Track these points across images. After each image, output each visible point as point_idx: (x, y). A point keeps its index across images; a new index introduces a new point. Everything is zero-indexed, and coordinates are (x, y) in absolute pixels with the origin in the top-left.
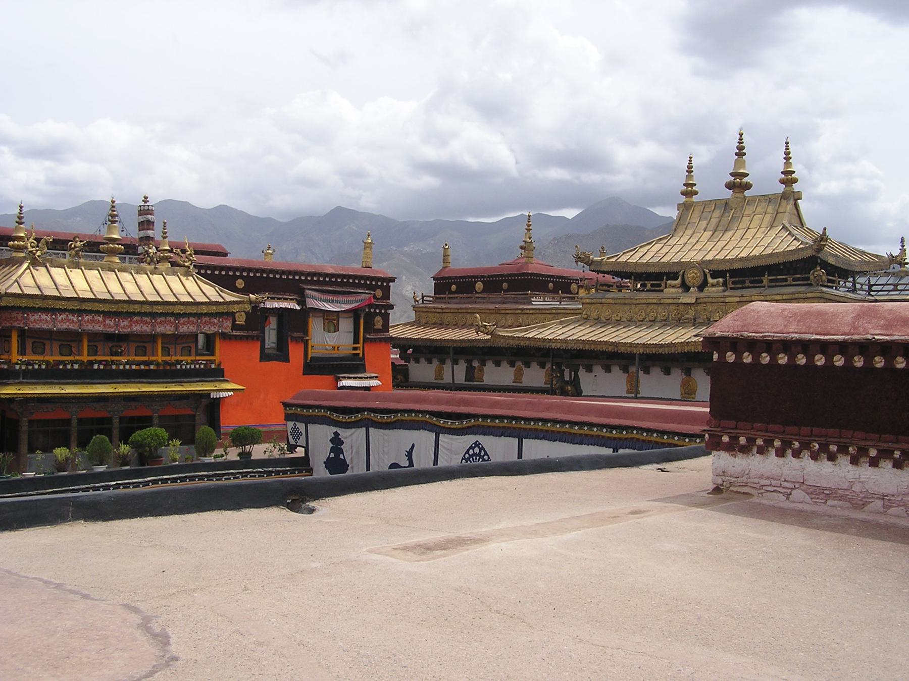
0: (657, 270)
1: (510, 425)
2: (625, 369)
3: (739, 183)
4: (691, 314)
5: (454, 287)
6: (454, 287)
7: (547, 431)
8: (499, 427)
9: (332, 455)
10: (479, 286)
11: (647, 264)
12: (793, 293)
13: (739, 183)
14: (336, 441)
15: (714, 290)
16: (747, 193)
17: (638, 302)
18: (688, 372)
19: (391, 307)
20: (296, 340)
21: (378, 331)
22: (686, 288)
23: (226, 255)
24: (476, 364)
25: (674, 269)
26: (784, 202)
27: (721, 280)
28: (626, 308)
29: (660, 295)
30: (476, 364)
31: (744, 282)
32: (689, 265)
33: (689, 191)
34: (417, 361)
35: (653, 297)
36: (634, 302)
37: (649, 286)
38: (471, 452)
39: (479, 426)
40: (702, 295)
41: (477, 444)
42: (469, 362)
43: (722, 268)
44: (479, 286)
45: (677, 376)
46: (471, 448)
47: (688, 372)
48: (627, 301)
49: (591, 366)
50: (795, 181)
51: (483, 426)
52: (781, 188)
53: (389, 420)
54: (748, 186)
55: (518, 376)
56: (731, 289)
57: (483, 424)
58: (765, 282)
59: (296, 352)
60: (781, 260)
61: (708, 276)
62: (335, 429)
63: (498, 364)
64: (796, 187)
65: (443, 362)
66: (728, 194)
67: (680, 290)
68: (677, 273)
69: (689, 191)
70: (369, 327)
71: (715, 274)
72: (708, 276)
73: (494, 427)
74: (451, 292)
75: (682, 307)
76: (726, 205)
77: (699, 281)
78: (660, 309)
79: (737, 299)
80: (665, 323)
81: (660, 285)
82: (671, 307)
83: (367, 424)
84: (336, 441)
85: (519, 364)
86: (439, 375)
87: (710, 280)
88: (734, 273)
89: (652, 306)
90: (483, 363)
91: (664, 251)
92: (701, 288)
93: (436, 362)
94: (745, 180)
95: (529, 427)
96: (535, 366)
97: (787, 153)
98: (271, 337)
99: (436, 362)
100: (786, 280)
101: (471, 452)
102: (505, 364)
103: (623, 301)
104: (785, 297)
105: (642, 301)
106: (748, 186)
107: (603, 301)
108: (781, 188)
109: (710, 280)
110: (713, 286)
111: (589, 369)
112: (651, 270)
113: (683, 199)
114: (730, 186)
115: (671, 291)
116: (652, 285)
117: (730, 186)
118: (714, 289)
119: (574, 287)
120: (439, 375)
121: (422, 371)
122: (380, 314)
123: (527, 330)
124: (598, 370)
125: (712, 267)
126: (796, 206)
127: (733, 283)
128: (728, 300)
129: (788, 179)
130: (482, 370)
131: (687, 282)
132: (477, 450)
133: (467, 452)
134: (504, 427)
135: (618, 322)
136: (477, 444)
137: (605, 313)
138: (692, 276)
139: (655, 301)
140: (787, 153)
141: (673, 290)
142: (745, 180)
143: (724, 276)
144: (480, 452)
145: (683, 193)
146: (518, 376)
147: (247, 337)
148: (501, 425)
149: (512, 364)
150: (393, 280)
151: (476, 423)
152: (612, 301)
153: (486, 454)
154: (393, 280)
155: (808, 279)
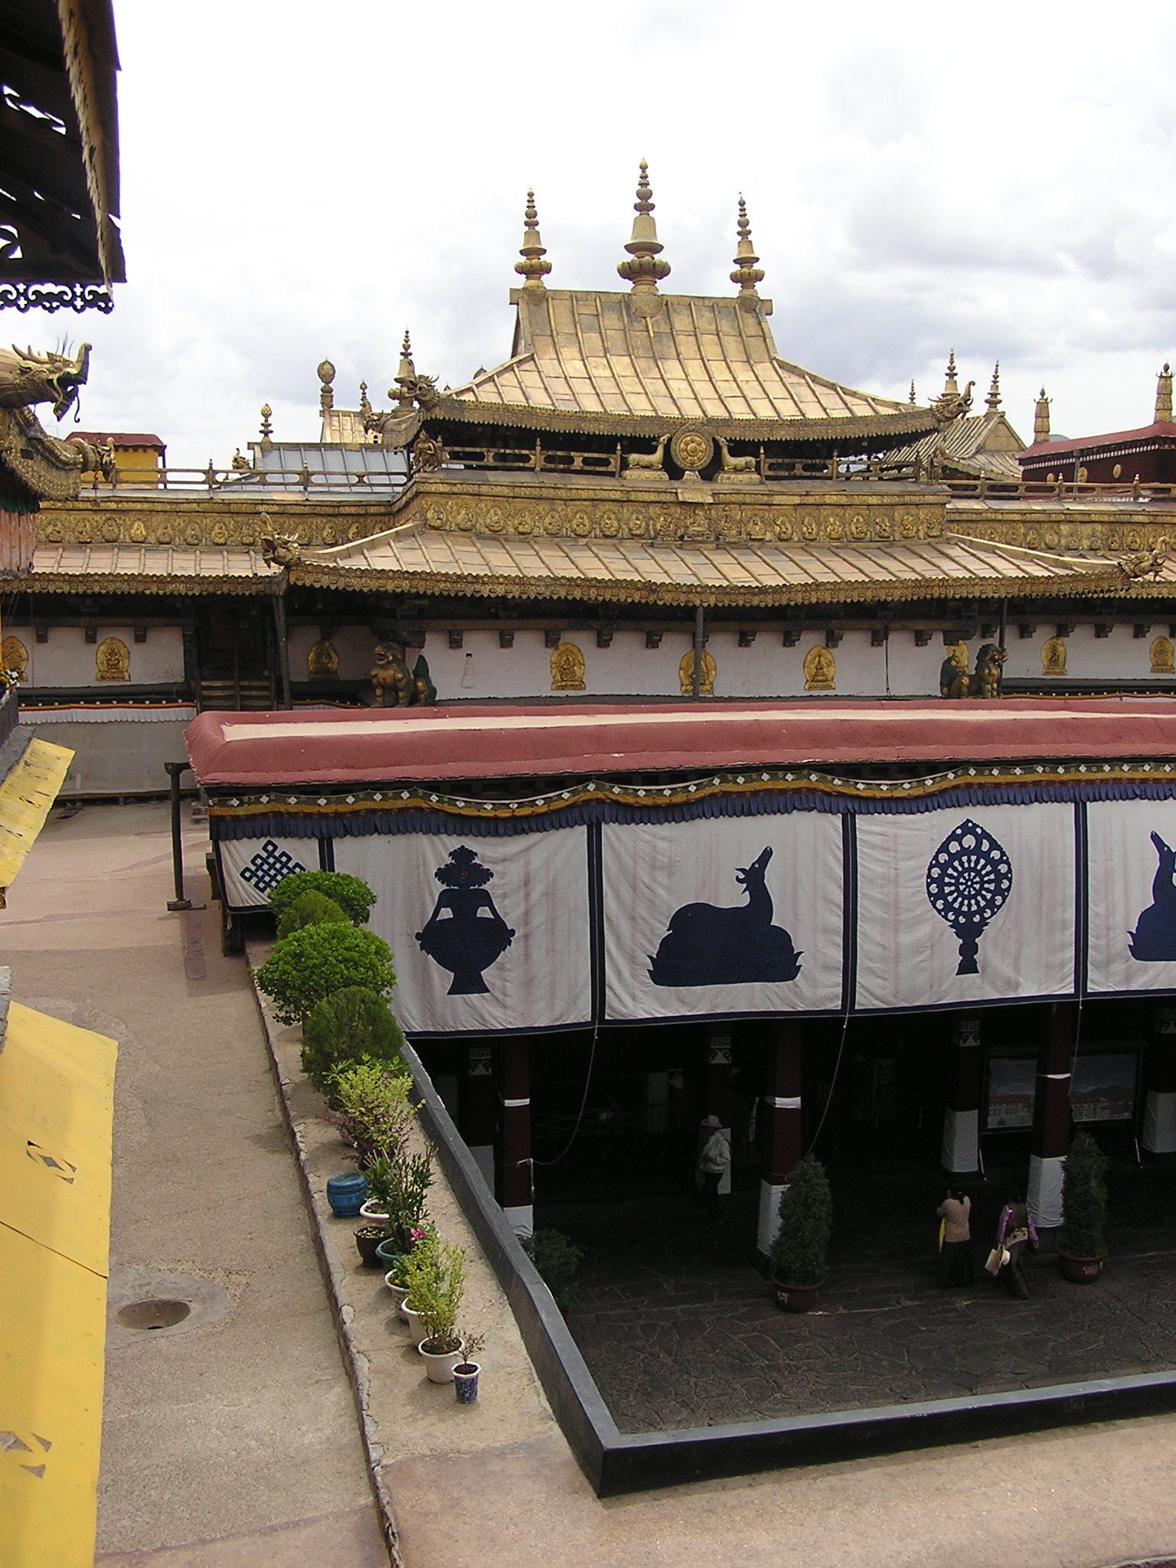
1: (1052, 777)
3: (644, 264)
7: (1143, 781)
8: (1023, 785)
9: (446, 913)
13: (644, 264)
14: (464, 880)
15: (740, 478)
16: (664, 286)
17: (574, 494)
22: (674, 471)
25: (646, 432)
27: (752, 460)
28: (542, 507)
31: (792, 467)
32: (680, 425)
33: (533, 264)
36: (563, 494)
37: (578, 463)
38: (954, 847)
39: (969, 785)
41: (968, 828)
43: (749, 436)
45: (674, 650)
46: (953, 837)
48: (545, 493)
49: (460, 633)
50: (759, 277)
51: (981, 785)
53: (679, 798)
54: (663, 271)
56: (768, 478)
57: (981, 780)
61: (725, 450)
62: (454, 843)
64: (762, 289)
66: (627, 286)
68: (654, 439)
71: (739, 448)
72: (725, 450)
73: (1009, 785)
75: (677, 511)
76: (625, 303)
77: (704, 458)
79: (797, 500)
80: (652, 541)
81: (607, 463)
82: (653, 510)
83: (592, 818)
84: (464, 880)
88: (775, 448)
89: (607, 506)
92: (708, 474)
95: (1099, 776)
97: (743, 224)
101: (954, 847)
103: (536, 492)
104: (886, 500)
105: (584, 495)
106: (663, 271)
107: (484, 489)
108: (734, 290)
110: (737, 470)
113: (520, 281)
114: (627, 272)
115: (643, 475)
116: (585, 461)
117: (627, 272)
118: (740, 477)
124: (480, 644)
125: (730, 433)
127: (771, 467)
128: (777, 499)
129: (747, 273)
131: (679, 459)
132: (969, 841)
133: (944, 848)
134: (1035, 783)
135: (525, 537)
136: (968, 828)
137: (581, 522)
138: (693, 449)
139: (617, 496)
140: (743, 224)
141: (647, 473)
143: (756, 455)
144: (979, 844)
145: (520, 270)
148: (1029, 778)
151: (961, 781)
152: (506, 491)
153: (994, 845)
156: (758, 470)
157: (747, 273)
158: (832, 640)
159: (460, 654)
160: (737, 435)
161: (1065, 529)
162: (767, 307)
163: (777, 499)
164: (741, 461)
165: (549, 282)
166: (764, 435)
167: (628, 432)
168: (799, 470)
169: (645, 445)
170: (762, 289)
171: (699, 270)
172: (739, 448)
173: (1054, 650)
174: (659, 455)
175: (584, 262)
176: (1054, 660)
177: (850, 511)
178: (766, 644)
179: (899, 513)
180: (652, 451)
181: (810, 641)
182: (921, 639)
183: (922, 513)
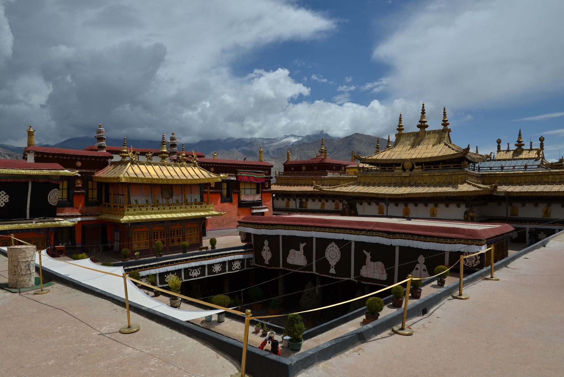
0: (391, 162)
2: (378, 204)
3: (422, 125)
4: (407, 180)
5: (292, 169)
6: (292, 169)
10: (304, 168)
11: (386, 160)
12: (454, 172)
13: (422, 125)
15: (417, 170)
16: (427, 129)
18: (406, 205)
19: (272, 178)
20: (235, 193)
21: (267, 188)
22: (404, 169)
23: (204, 157)
24: (304, 200)
26: (444, 133)
28: (377, 178)
29: (393, 173)
30: (304, 200)
32: (405, 160)
33: (400, 128)
34: (277, 199)
35: (390, 174)
40: (412, 173)
42: (301, 200)
43: (420, 161)
44: (304, 168)
45: (401, 207)
47: (406, 205)
50: (448, 124)
52: (442, 127)
55: (323, 205)
58: (440, 167)
59: (235, 198)
60: (448, 158)
63: (314, 201)
64: (449, 127)
65: (289, 200)
66: (418, 130)
67: (402, 171)
69: (400, 128)
70: (264, 187)
71: (418, 164)
74: (292, 171)
75: (403, 178)
76: (416, 135)
78: (393, 178)
80: (396, 185)
82: (398, 178)
85: (323, 201)
86: (287, 204)
87: (416, 167)
90: (307, 200)
91: (392, 154)
92: (412, 169)
93: (286, 200)
94: (426, 124)
96: (330, 201)
97: (445, 113)
98: (225, 192)
99: (286, 200)
100: (450, 166)
102: (317, 201)
108: (442, 127)
109: (416, 167)
111: (361, 204)
112: (388, 162)
113: (397, 132)
114: (418, 126)
115: (398, 171)
119: (343, 168)
120: (287, 204)
121: (281, 203)
122: (267, 181)
123: (334, 188)
124: (365, 204)
126: (449, 135)
127: (426, 168)
128: (424, 175)
129: (445, 123)
130: (306, 203)
138: (408, 165)
140: (445, 113)
141: (398, 171)
142: (426, 124)
146: (323, 205)
147: (215, 193)
149: (320, 201)
150: (272, 166)
154: (272, 166)
155: (460, 166)
156: (422, 168)
157: (445, 123)
158: (436, 206)
159: (362, 206)
160: (417, 161)
161: (550, 177)
162: (449, 131)
163: (424, 175)
164: (417, 167)
165: (403, 132)
166: (423, 161)
167: (395, 162)
168: (432, 168)
169: (399, 165)
170: (449, 127)
171: (434, 125)
172: (418, 164)
173: (547, 210)
174: (401, 167)
175: (412, 127)
176: (546, 213)
177: (441, 177)
178: (421, 206)
179: (454, 177)
180: (400, 166)
181: (431, 206)
182: (458, 206)
183: (460, 176)
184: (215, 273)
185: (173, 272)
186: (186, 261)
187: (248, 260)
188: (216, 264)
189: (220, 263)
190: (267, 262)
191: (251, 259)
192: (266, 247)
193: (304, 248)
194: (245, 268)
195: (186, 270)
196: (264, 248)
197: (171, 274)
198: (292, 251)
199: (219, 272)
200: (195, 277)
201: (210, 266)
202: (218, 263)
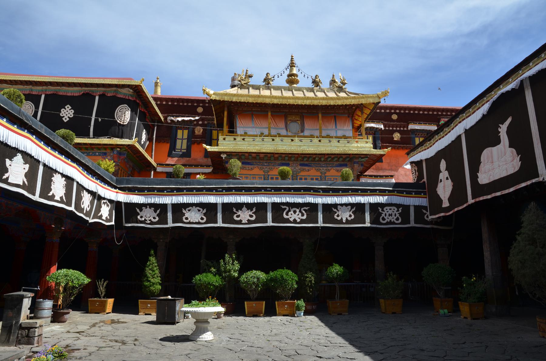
184: (341, 222)
185: (249, 206)
186: (277, 191)
187: (418, 209)
188: (342, 205)
189: (352, 205)
190: (446, 204)
191: (425, 208)
192: (444, 174)
193: (508, 132)
194: (412, 224)
195: (276, 207)
196: (441, 176)
197: (244, 208)
198: (486, 153)
199: (348, 222)
200: (295, 221)
201: (329, 209)
202: (346, 205)
